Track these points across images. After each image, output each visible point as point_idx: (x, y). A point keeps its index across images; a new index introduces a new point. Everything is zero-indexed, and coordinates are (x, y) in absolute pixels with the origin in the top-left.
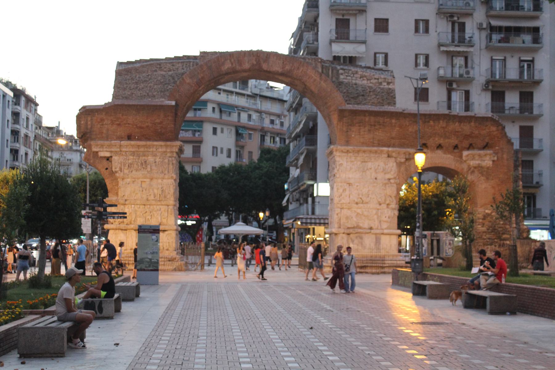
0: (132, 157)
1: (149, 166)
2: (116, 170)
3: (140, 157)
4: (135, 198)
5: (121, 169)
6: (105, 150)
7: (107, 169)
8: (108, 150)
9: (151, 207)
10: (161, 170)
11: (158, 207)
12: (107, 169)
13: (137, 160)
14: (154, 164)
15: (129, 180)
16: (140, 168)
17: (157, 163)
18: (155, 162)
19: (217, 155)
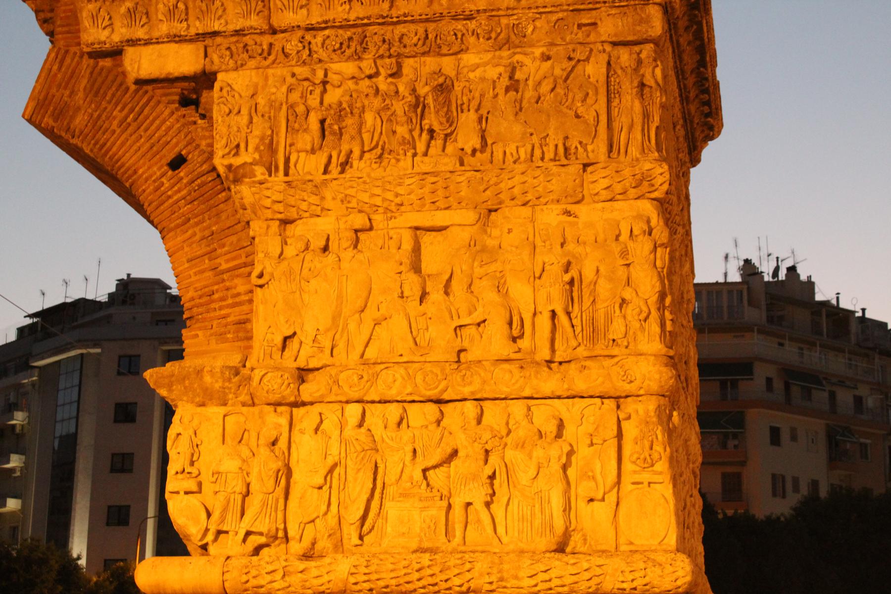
0: (349, 68)
1: (468, 120)
2: (237, 161)
3: (409, 65)
4: (371, 354)
5: (272, 148)
6: (164, 29)
7: (177, 163)
8: (180, 28)
9: (493, 414)
10: (555, 138)
11: (543, 415)
12: (177, 163)
13: (382, 83)
14: (504, 101)
15: (325, 225)
16: (402, 130)
17: (529, 94)
18: (514, 86)
19: (784, 497)
